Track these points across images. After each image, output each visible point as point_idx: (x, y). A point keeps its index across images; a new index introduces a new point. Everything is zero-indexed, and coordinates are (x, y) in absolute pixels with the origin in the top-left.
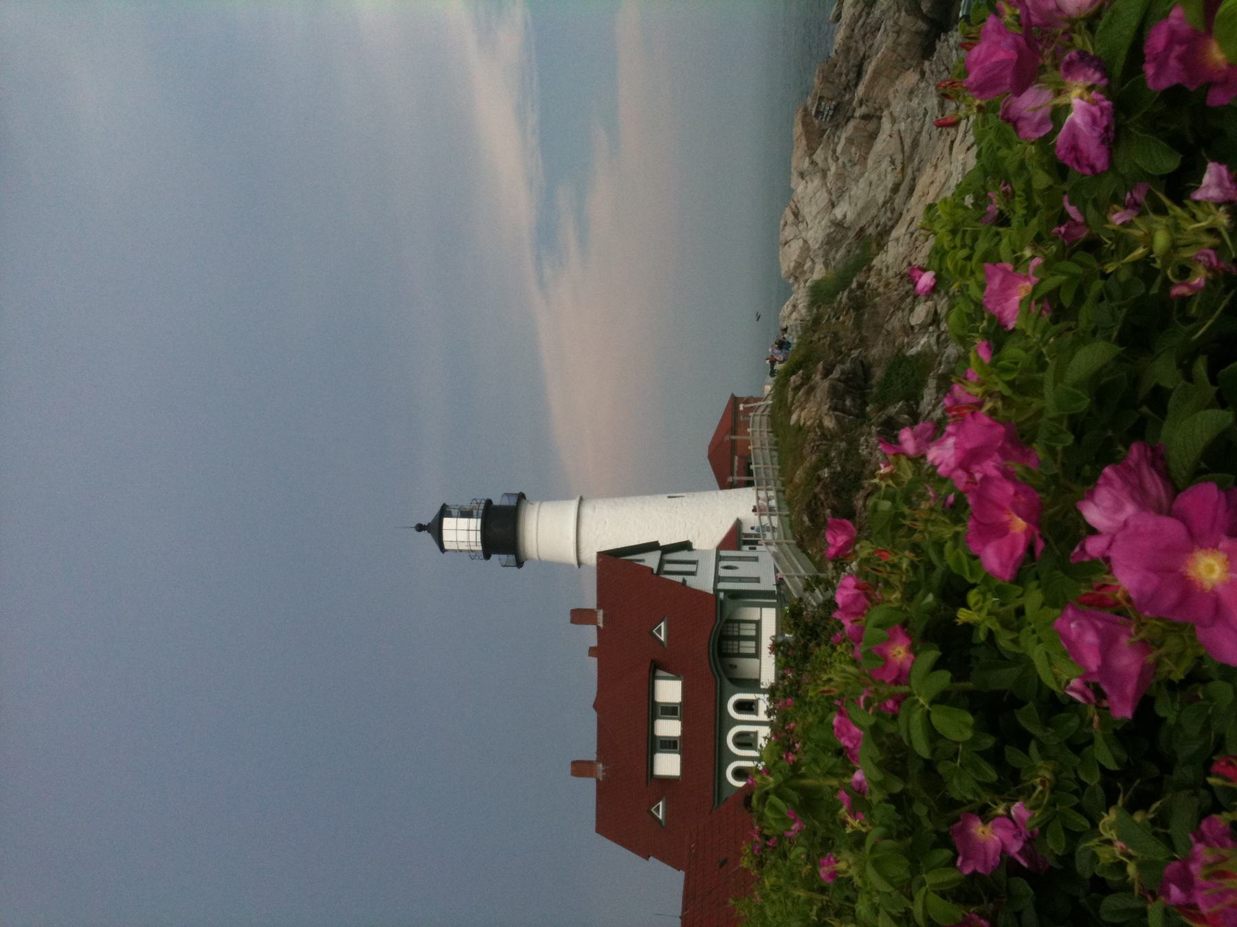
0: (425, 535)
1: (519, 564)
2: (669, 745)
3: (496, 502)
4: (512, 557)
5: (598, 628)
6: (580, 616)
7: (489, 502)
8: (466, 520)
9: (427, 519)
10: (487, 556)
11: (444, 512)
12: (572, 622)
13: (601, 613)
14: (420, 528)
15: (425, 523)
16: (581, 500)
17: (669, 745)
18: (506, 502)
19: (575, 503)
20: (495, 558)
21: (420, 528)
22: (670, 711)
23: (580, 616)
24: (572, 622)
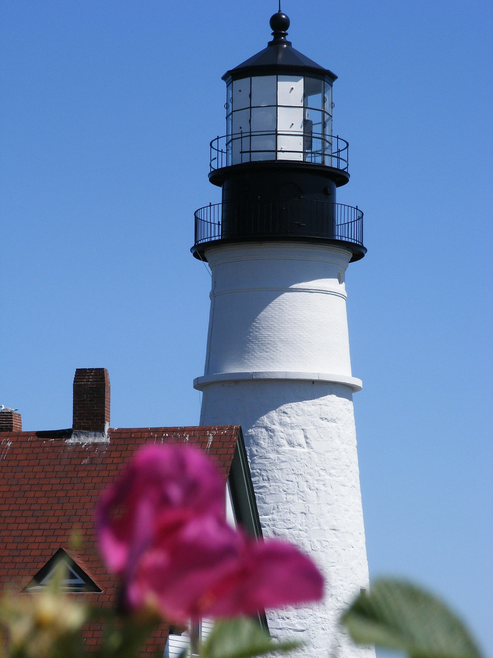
5: (66, 434)
6: (91, 391)
8: (299, 128)
11: (317, 78)
12: (80, 373)
13: (105, 439)
14: (279, 24)
15: (292, 35)
19: (342, 372)
21: (279, 24)
23: (91, 391)
24: (80, 373)
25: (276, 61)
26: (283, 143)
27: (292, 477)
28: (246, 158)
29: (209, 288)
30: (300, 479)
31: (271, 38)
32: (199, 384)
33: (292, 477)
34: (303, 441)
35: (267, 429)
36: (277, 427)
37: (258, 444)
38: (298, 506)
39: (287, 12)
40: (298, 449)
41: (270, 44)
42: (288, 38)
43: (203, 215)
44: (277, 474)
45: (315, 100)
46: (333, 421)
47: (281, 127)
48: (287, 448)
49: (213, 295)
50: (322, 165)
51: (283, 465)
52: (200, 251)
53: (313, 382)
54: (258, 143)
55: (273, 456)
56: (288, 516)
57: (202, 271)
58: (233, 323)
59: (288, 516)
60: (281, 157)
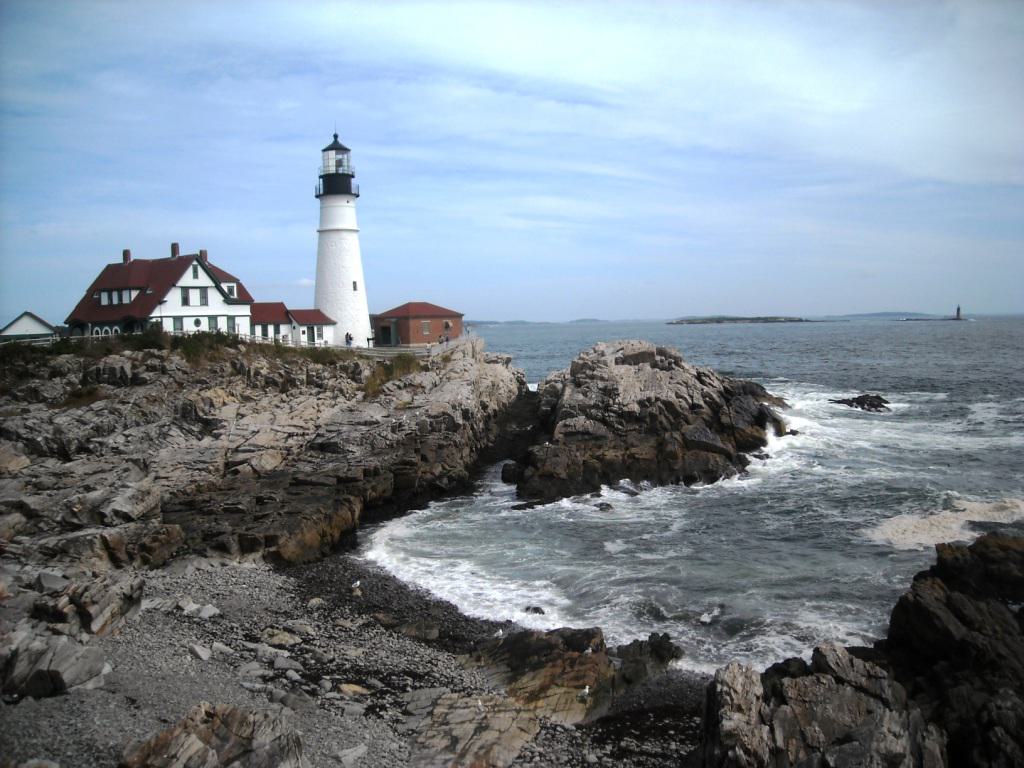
0: (331, 140)
1: (317, 197)
2: (110, 298)
3: (353, 181)
4: (322, 192)
6: (175, 248)
7: (353, 176)
9: (341, 141)
10: (321, 177)
14: (336, 136)
15: (339, 139)
16: (357, 231)
17: (110, 298)
21: (336, 136)
22: (120, 299)
23: (175, 248)
49: (321, 208)
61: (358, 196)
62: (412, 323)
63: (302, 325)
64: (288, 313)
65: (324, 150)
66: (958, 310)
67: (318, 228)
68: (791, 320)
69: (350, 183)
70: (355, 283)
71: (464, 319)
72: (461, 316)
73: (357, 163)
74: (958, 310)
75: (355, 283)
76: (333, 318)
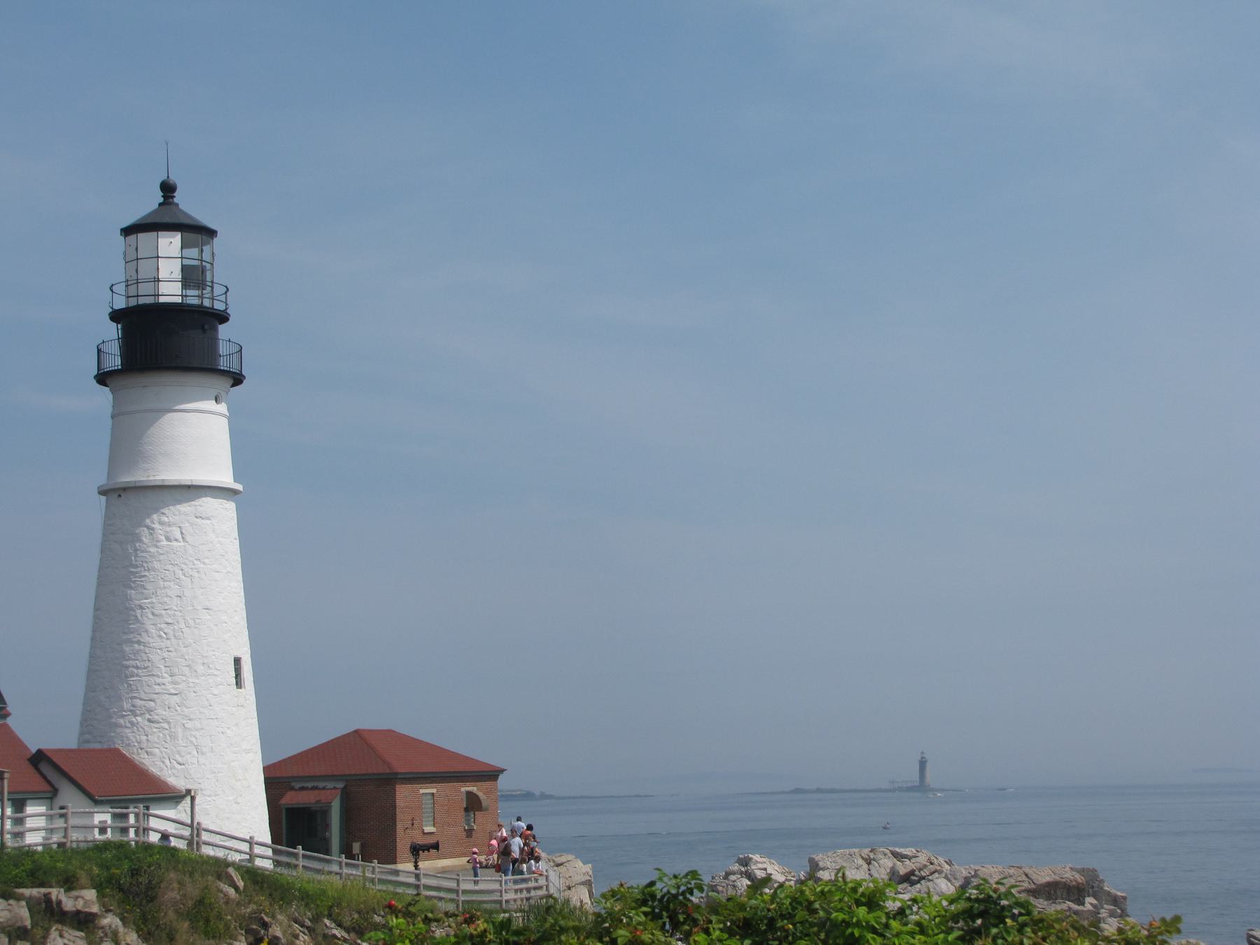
3: (223, 330)
7: (223, 318)
8: (178, 275)
9: (189, 204)
10: (116, 316)
14: (168, 189)
15: (178, 197)
16: (234, 492)
18: (223, 349)
19: (226, 478)
20: (112, 331)
21: (168, 189)
25: (165, 218)
26: (164, 288)
27: (170, 567)
28: (133, 302)
29: (110, 409)
30: (176, 569)
31: (161, 200)
32: (103, 492)
33: (170, 567)
34: (179, 536)
35: (148, 527)
36: (157, 526)
37: (141, 541)
38: (174, 590)
39: (174, 178)
40: (175, 544)
41: (160, 205)
42: (175, 200)
43: (105, 348)
44: (156, 565)
45: (193, 252)
46: (208, 518)
47: (163, 274)
48: (165, 543)
50: (201, 306)
51: (161, 557)
52: (103, 378)
53: (189, 487)
54: (145, 289)
55: (152, 550)
56: (165, 599)
57: (104, 396)
58: (127, 440)
59: (165, 599)
60: (162, 300)
61: (237, 379)
62: (403, 793)
63: (97, 802)
64: (39, 759)
65: (128, 231)
66: (923, 764)
67: (102, 480)
68: (833, 791)
69: (216, 330)
70: (237, 661)
71: (503, 782)
72: (491, 774)
73: (238, 280)
74: (923, 764)
75: (237, 661)
76: (177, 781)
